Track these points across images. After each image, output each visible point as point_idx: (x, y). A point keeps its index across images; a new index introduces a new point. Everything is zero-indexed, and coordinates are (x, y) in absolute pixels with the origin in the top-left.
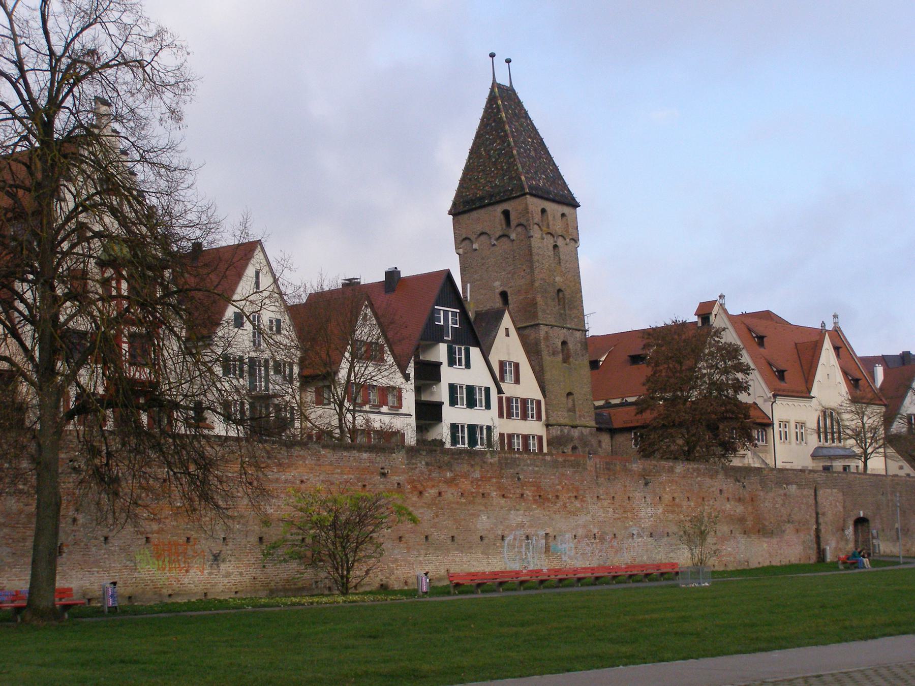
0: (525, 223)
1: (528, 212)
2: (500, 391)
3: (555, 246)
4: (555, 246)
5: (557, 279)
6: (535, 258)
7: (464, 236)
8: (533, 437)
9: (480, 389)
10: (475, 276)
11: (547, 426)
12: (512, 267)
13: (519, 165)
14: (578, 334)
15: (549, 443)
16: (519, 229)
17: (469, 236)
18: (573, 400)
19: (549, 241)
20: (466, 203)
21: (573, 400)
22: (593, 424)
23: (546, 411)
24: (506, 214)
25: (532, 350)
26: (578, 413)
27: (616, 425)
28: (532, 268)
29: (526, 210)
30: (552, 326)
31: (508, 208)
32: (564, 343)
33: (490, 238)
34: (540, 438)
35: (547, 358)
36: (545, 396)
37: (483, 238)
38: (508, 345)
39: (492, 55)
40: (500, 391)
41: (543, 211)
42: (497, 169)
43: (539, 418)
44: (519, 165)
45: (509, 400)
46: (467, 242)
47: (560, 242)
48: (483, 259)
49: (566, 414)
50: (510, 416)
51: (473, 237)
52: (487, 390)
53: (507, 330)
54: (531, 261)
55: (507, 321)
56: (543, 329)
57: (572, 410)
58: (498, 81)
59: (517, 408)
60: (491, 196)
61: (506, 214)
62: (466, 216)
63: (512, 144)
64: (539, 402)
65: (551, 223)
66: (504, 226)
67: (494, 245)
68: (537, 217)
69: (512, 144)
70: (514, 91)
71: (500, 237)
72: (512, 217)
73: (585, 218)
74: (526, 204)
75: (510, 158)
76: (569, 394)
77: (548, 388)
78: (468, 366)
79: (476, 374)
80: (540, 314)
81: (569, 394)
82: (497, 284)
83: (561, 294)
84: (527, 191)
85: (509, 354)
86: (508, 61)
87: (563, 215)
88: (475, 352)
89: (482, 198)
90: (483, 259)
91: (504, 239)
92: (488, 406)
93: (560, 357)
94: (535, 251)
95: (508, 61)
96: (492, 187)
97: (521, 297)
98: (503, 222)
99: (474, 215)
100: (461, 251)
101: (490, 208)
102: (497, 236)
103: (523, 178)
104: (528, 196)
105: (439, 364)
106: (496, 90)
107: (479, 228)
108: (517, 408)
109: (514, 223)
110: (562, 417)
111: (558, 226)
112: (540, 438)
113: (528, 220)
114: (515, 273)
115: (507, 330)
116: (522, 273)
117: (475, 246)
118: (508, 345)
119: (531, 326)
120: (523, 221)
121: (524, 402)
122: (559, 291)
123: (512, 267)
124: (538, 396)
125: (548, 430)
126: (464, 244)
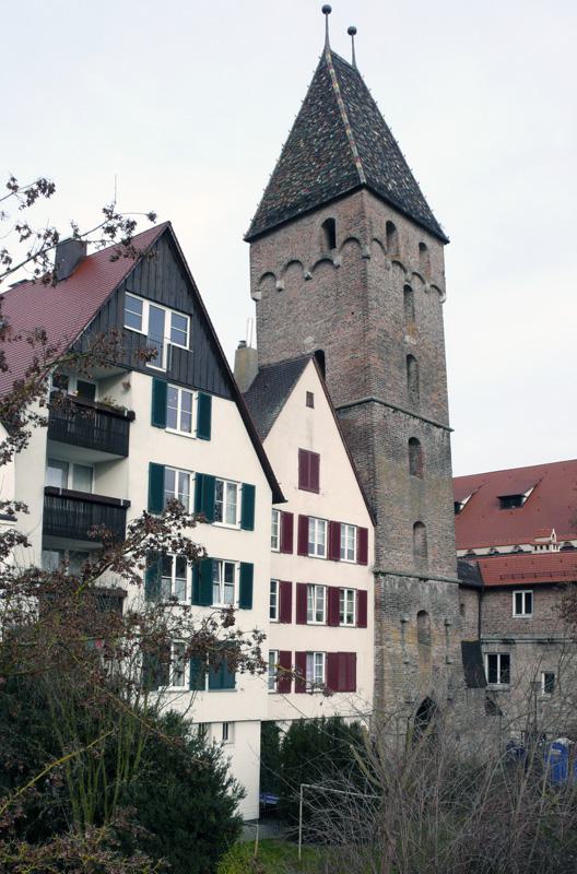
0: (358, 236)
1: (364, 217)
2: (278, 497)
3: (408, 289)
4: (408, 289)
5: (407, 338)
6: (372, 294)
7: (264, 271)
8: (350, 592)
9: (232, 487)
10: (278, 332)
11: (376, 574)
12: (334, 310)
13: (354, 149)
14: (438, 432)
15: (378, 605)
16: (349, 247)
17: (272, 270)
18: (425, 537)
19: (397, 278)
20: (271, 218)
21: (425, 537)
22: (454, 576)
23: (377, 549)
24: (329, 226)
25: (356, 442)
26: (431, 558)
27: (487, 583)
28: (366, 310)
29: (362, 214)
30: (396, 409)
31: (332, 216)
32: (413, 441)
33: (303, 269)
34: (363, 595)
35: (383, 460)
36: (375, 524)
37: (294, 269)
38: (305, 421)
39: (327, 10)
40: (278, 497)
41: (390, 227)
42: (319, 161)
43: (363, 559)
44: (354, 149)
45: (304, 521)
46: (268, 280)
47: (416, 285)
48: (290, 303)
49: (411, 557)
50: (304, 549)
51: (277, 271)
52: (249, 491)
53: (310, 396)
54: (364, 298)
55: (309, 379)
56: (378, 413)
57: (422, 553)
58: (334, 48)
59: (318, 535)
60: (306, 199)
61: (329, 226)
62: (268, 240)
63: (346, 121)
64: (363, 533)
65: (402, 249)
66: (326, 248)
67: (308, 279)
68: (380, 232)
69: (346, 121)
70: (356, 71)
71: (319, 263)
72: (338, 229)
73: (455, 261)
74: (362, 203)
75: (341, 142)
76: (418, 524)
77: (383, 509)
78: (204, 431)
79: (225, 451)
80: (374, 385)
81: (418, 524)
82: (309, 340)
83: (413, 364)
84: (364, 181)
85: (311, 440)
86: (352, 32)
87: (422, 247)
88: (224, 412)
89: (295, 206)
90: (290, 303)
91: (325, 268)
92: (248, 522)
93: (406, 464)
94: (372, 282)
95: (352, 32)
96: (309, 189)
97: (348, 358)
98: (325, 241)
99: (281, 235)
100: (259, 295)
101: (305, 221)
102: (313, 263)
103: (359, 165)
104: (364, 192)
105: (131, 416)
106: (329, 57)
107: (287, 256)
108: (318, 535)
109: (340, 238)
110: (402, 560)
111: (412, 259)
112: (363, 595)
113: (363, 230)
114: (337, 320)
115: (310, 396)
116: (350, 319)
117: (279, 284)
118: (305, 421)
119: (360, 403)
120: (355, 233)
121: (335, 529)
122: (410, 358)
123: (334, 310)
124: (365, 521)
125: (377, 582)
126: (264, 283)
